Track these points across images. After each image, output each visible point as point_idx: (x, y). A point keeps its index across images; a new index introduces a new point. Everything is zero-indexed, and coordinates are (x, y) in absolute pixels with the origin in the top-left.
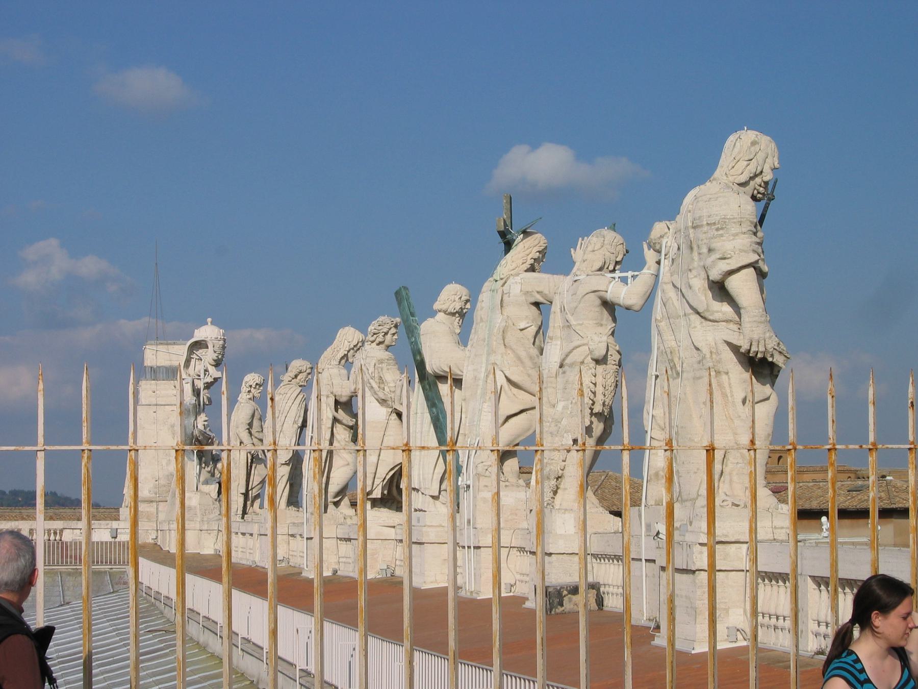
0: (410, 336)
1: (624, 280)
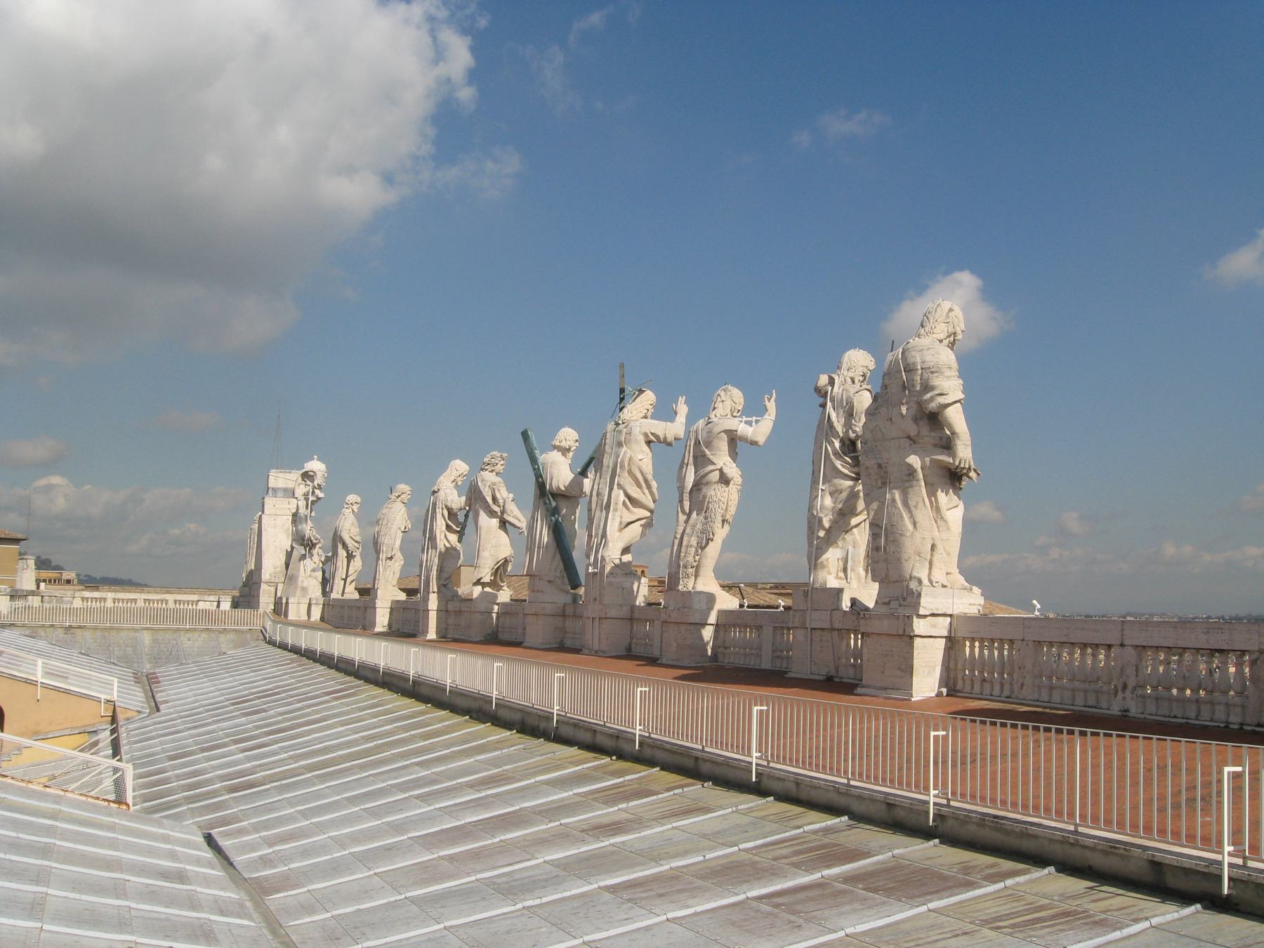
1: (749, 423)
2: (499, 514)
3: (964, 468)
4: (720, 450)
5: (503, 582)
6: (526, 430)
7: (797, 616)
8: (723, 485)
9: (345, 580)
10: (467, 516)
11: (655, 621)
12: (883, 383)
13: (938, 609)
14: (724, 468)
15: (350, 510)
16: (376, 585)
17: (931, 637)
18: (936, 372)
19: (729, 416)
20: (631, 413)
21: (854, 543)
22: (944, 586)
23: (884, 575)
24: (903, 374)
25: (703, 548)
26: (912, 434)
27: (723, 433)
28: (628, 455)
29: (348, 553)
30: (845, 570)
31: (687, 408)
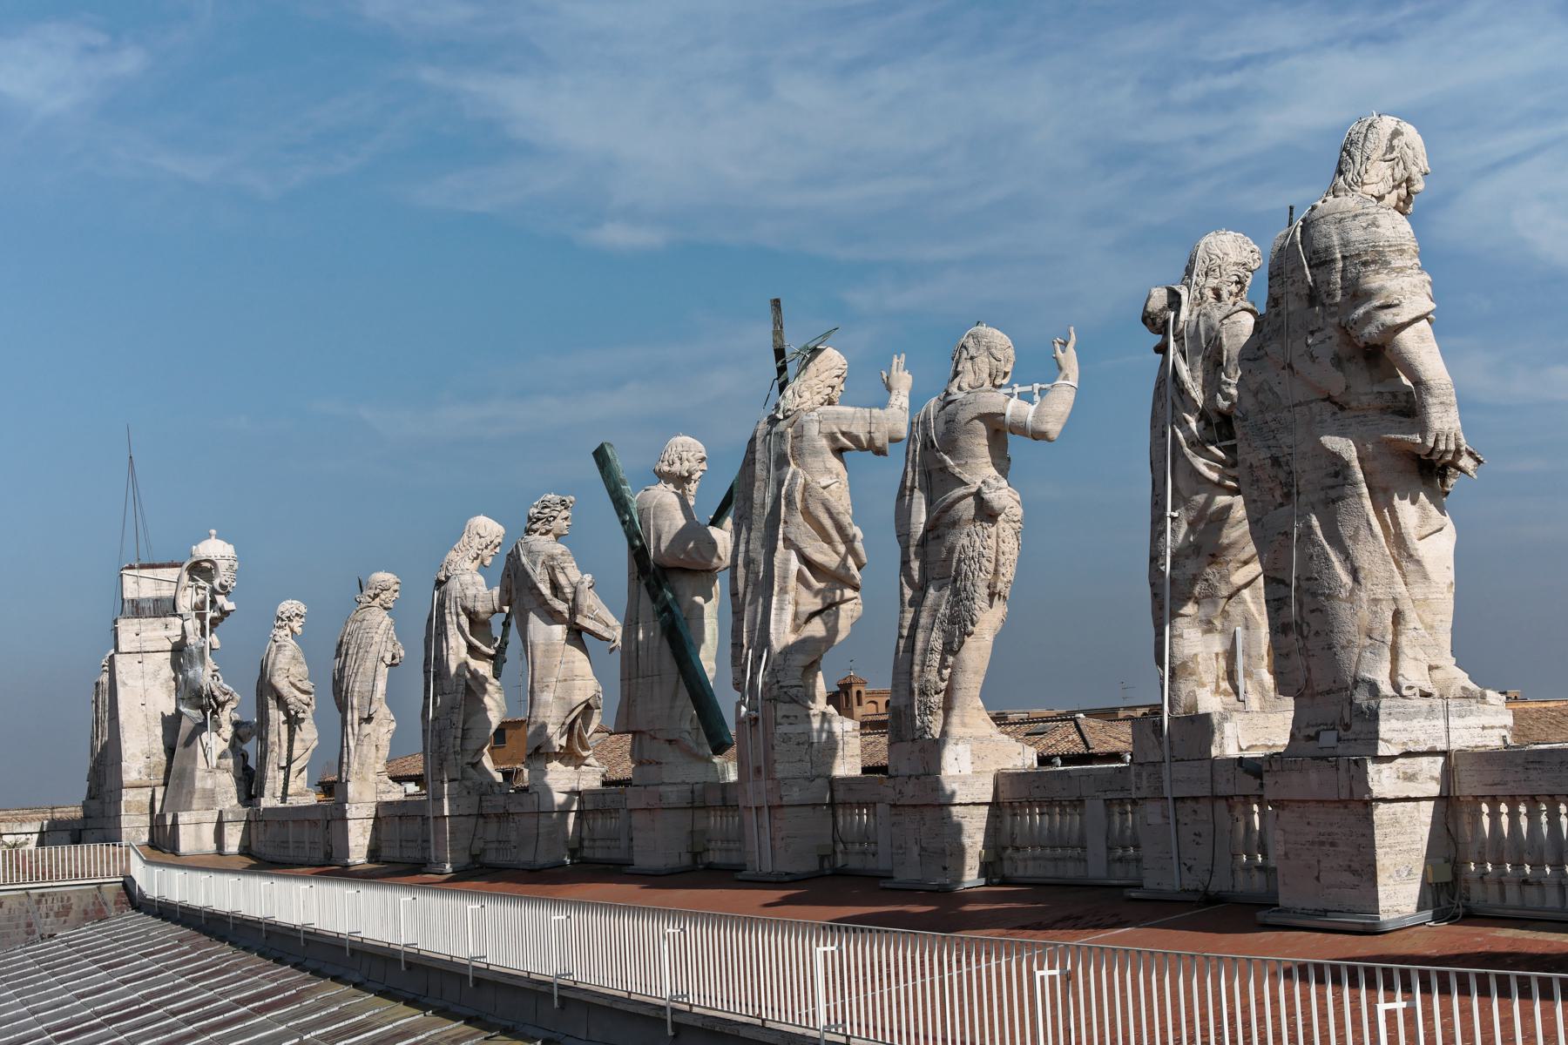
0: (622, 512)
1: (1027, 397)
2: (567, 616)
3: (1447, 451)
4: (974, 456)
5: (586, 748)
6: (602, 446)
7: (1144, 775)
8: (985, 525)
9: (287, 769)
10: (506, 625)
11: (878, 805)
12: (1270, 295)
13: (1416, 742)
14: (985, 489)
15: (288, 631)
16: (344, 775)
17: (1408, 799)
18: (1374, 262)
19: (987, 385)
20: (800, 397)
22: (1426, 695)
23: (1302, 682)
24: (1307, 271)
25: (955, 653)
26: (1336, 391)
27: (977, 421)
28: (800, 481)
29: (287, 713)
30: (1231, 675)
31: (910, 377)
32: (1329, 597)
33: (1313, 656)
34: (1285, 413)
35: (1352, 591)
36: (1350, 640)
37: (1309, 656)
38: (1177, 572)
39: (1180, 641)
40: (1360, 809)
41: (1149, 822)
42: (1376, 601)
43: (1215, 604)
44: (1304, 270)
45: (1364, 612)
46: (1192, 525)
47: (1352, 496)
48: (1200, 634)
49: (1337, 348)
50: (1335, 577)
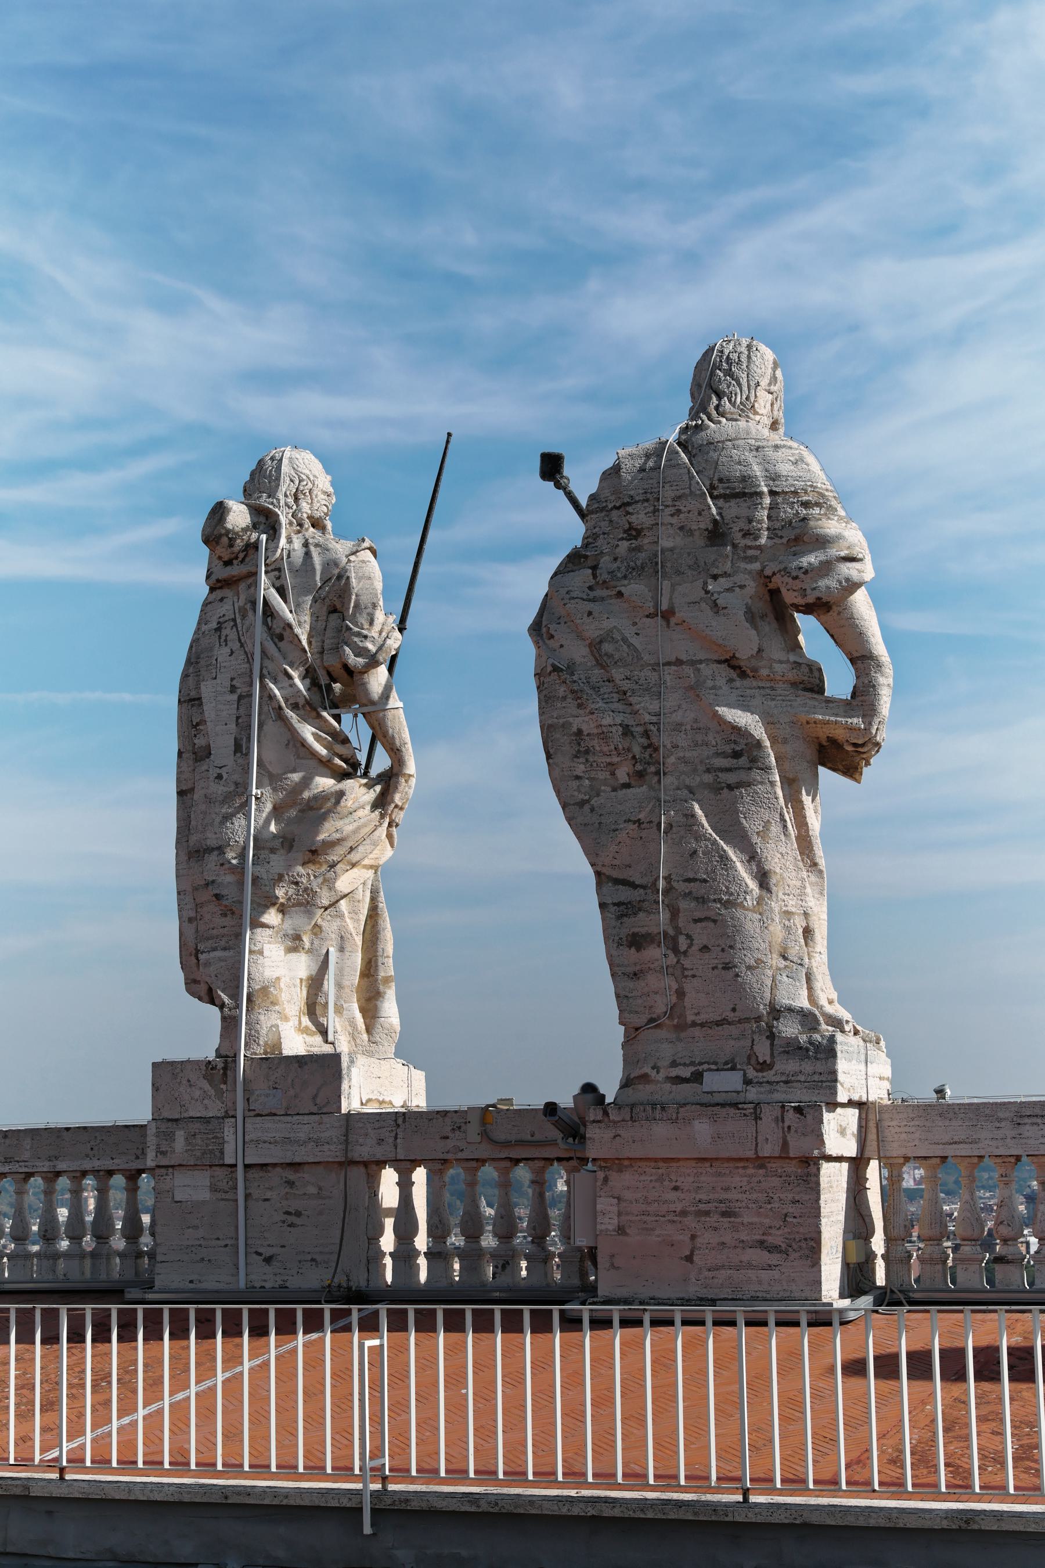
18: (818, 504)
21: (342, 937)
24: (709, 499)
32: (728, 904)
33: (694, 976)
34: (647, 672)
35: (760, 900)
36: (758, 959)
37: (686, 977)
38: (259, 868)
39: (261, 960)
40: (792, 1168)
41: (177, 1198)
42: (788, 914)
43: (310, 914)
44: (706, 499)
45: (777, 930)
46: (277, 811)
47: (762, 783)
48: (282, 953)
49: (750, 601)
50: (736, 879)
